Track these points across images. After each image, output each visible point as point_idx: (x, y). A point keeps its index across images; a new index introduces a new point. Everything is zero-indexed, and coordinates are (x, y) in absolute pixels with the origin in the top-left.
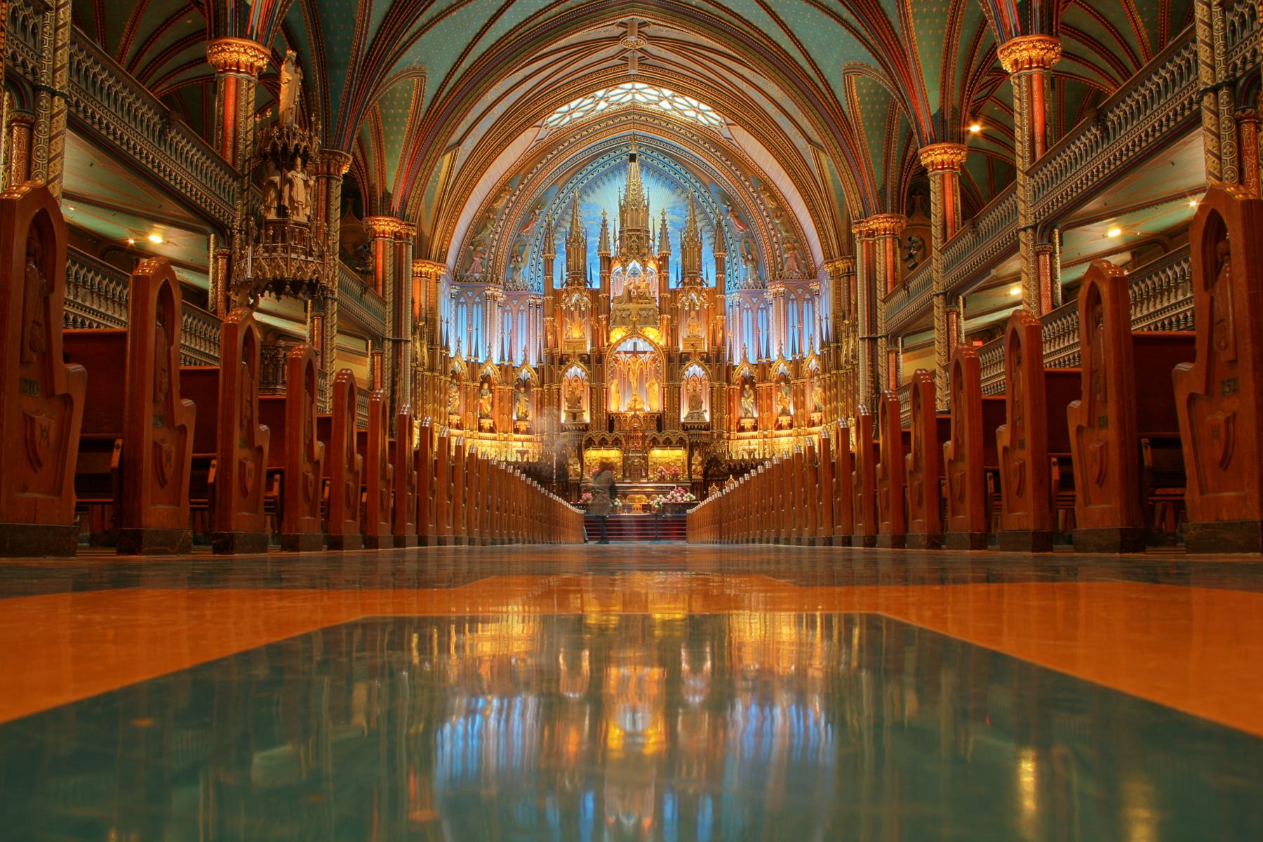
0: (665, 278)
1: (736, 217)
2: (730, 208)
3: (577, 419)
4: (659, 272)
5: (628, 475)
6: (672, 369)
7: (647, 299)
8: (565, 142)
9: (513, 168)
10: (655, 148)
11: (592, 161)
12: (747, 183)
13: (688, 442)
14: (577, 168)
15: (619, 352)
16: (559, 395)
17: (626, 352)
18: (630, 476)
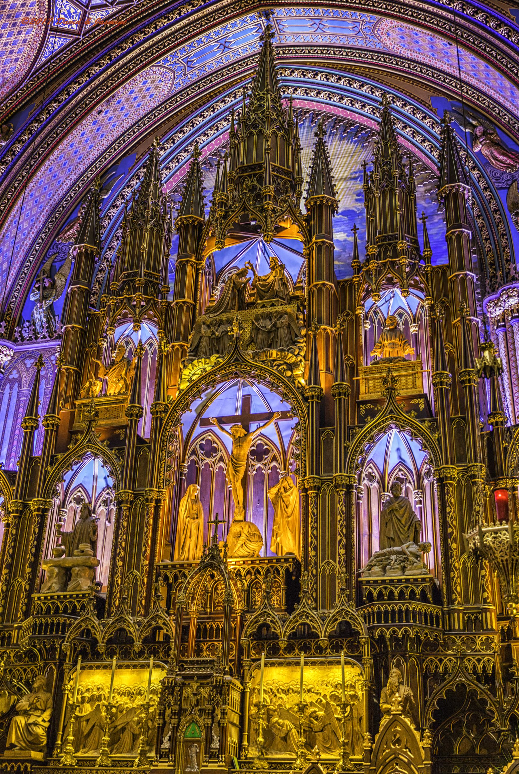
0: (320, 249)
1: (494, 144)
2: (479, 131)
3: (71, 585)
4: (307, 242)
5: (166, 745)
6: (329, 442)
7: (277, 296)
8: (125, 41)
9: (18, 92)
10: (320, 65)
11: (200, 106)
12: (502, 31)
13: (364, 636)
14: (173, 122)
15: (205, 422)
16: (42, 526)
17: (221, 421)
18: (172, 750)
